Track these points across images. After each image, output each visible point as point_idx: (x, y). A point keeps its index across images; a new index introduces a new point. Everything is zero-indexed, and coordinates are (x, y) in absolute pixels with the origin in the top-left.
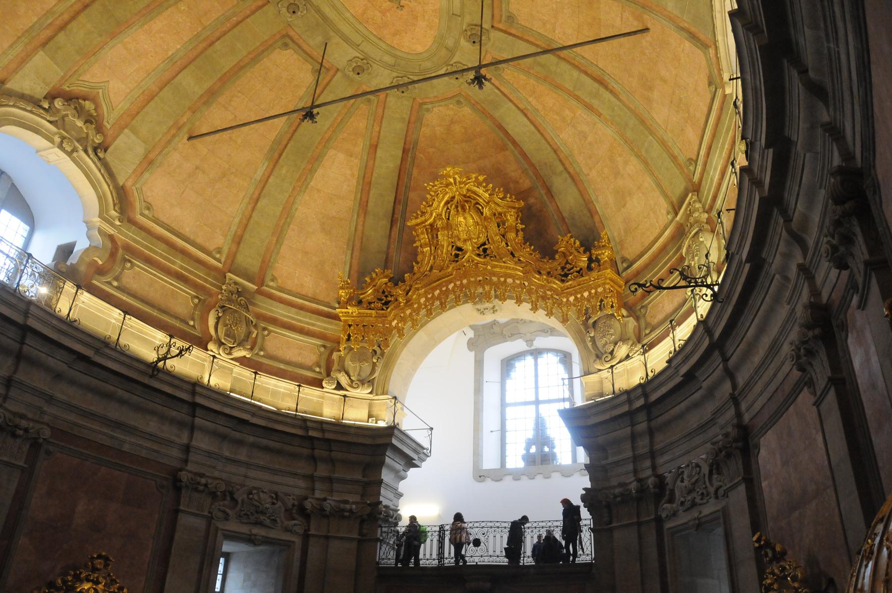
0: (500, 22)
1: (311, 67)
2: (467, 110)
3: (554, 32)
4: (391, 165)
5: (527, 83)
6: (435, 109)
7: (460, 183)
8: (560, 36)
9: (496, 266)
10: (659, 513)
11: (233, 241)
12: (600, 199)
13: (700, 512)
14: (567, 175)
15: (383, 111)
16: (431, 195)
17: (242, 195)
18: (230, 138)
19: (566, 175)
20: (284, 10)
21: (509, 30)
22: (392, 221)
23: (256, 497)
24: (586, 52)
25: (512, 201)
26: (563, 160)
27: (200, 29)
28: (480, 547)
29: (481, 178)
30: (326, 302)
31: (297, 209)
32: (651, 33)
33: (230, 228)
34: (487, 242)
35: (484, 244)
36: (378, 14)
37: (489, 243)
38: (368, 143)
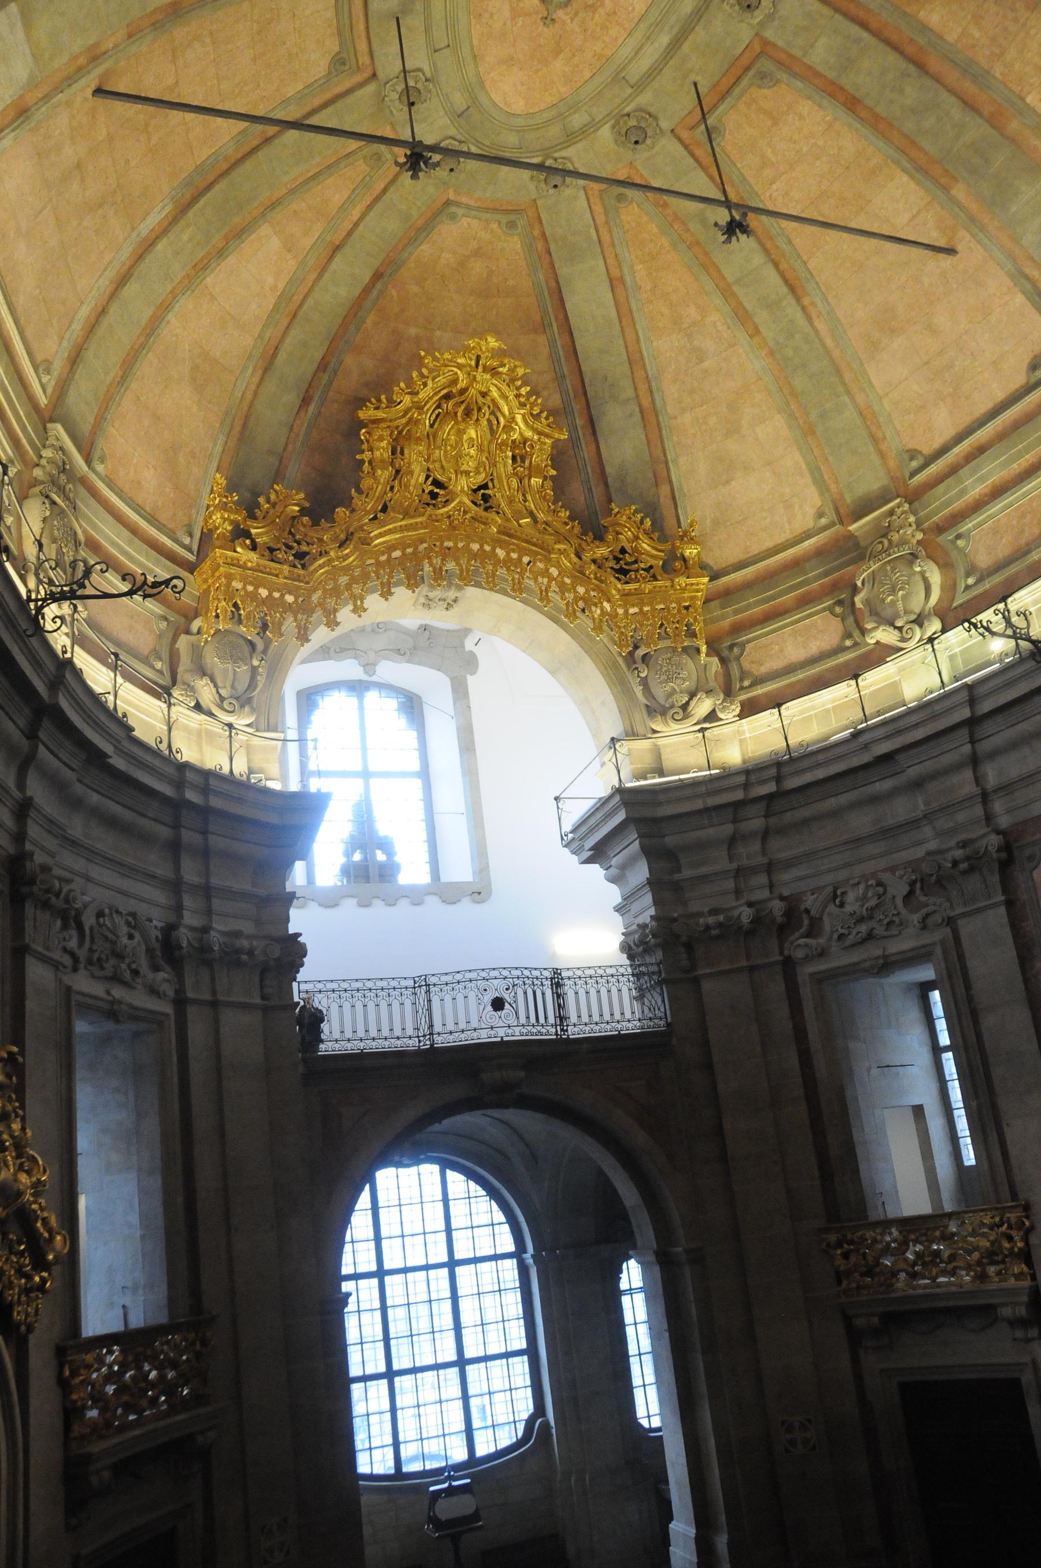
1: (337, 49)
2: (513, 245)
3: (771, 184)
6: (465, 221)
8: (775, 194)
10: (786, 953)
12: (682, 461)
14: (637, 409)
16: (422, 376)
18: (147, 125)
21: (691, 147)
23: (107, 922)
24: (801, 236)
25: (548, 425)
26: (636, 380)
28: (504, 1012)
29: (520, 371)
30: (170, 530)
34: (490, 485)
35: (485, 486)
36: (507, 12)
37: (494, 487)
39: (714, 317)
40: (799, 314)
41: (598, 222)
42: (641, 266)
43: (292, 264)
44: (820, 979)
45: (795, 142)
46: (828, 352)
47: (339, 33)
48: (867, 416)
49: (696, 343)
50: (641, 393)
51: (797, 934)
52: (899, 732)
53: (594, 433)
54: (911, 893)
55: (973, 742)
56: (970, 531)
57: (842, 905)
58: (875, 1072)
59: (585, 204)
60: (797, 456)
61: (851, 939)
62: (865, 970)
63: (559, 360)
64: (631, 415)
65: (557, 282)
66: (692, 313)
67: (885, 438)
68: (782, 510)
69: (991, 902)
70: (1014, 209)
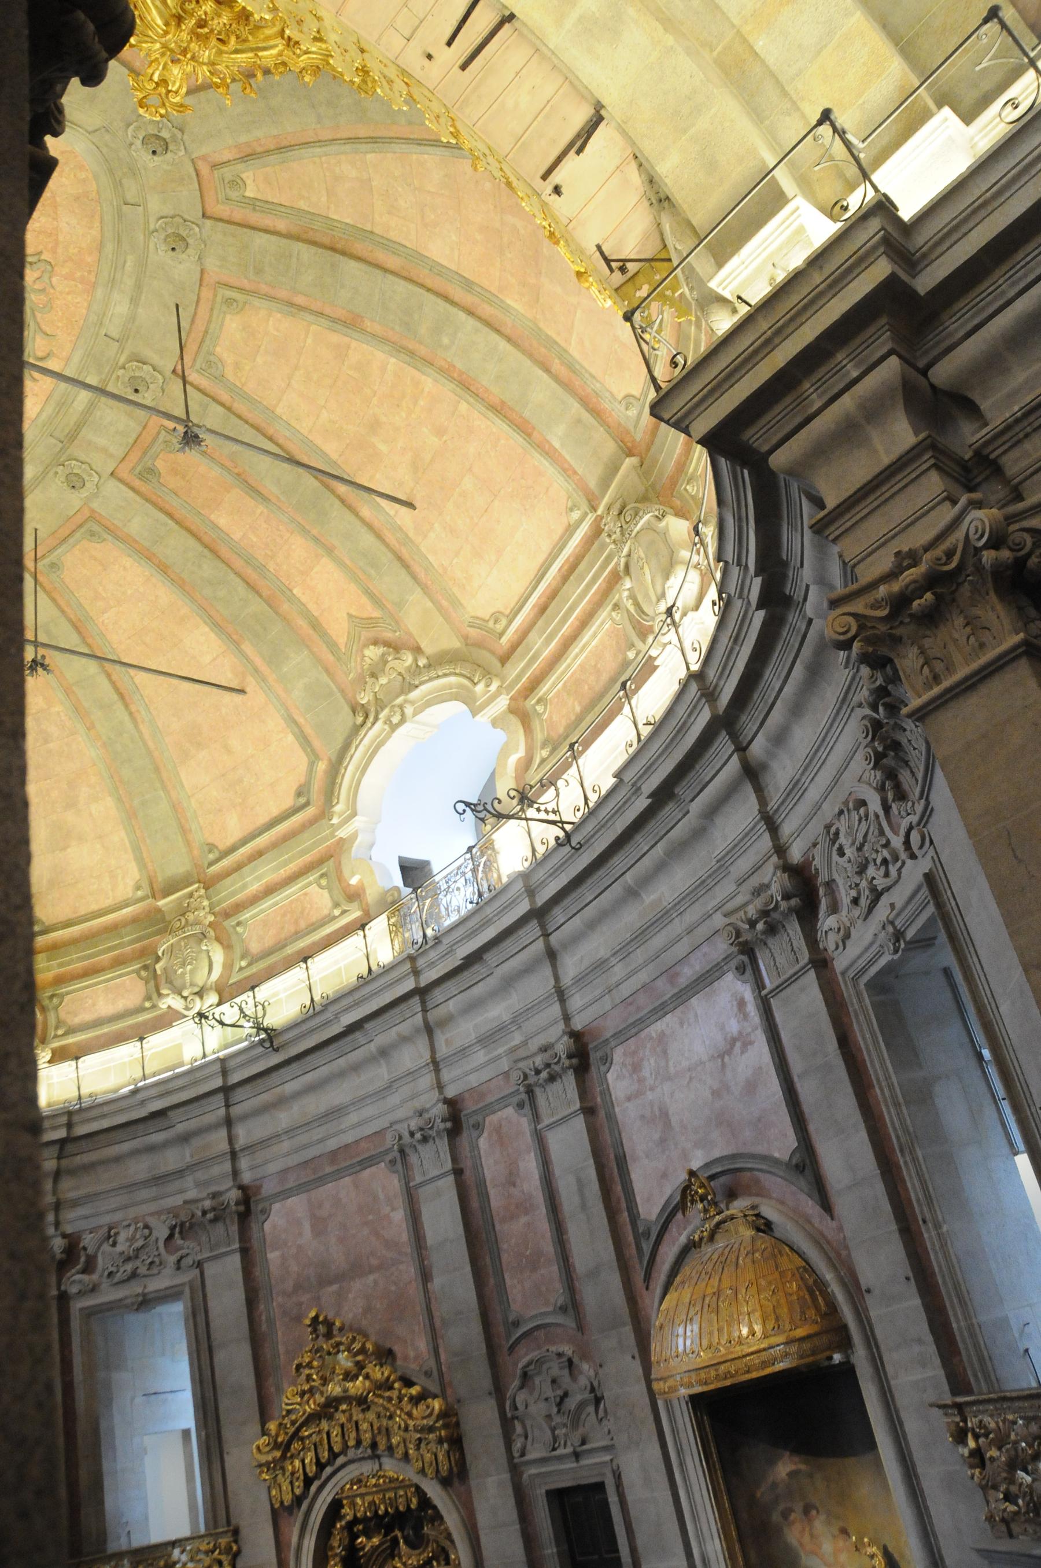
10: (63, 1288)
13: (145, 1287)
39: (57, 708)
40: (127, 718)
44: (89, 1313)
45: (121, 585)
46: (149, 753)
51: (73, 1271)
52: (168, 1093)
54: (170, 1237)
55: (227, 1106)
56: (247, 920)
57: (114, 1244)
58: (139, 1400)
60: (123, 834)
61: (118, 1277)
62: (126, 1306)
69: (228, 1249)
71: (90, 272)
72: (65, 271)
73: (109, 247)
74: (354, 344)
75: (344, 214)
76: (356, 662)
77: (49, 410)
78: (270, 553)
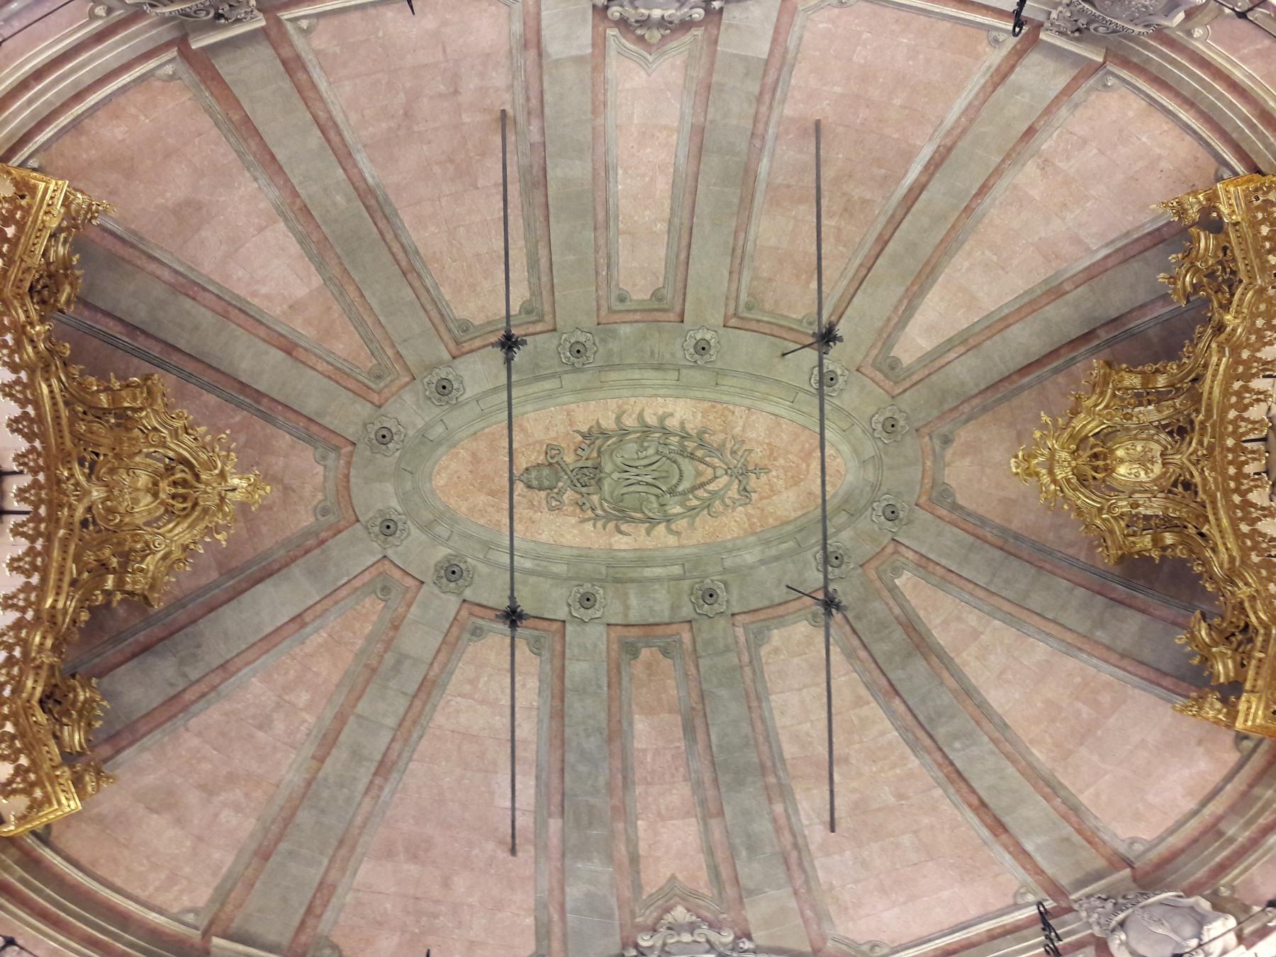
0: (471, 614)
2: (306, 519)
3: (459, 696)
4: (244, 365)
5: (354, 633)
6: (320, 469)
7: (222, 499)
8: (453, 703)
9: (64, 550)
11: (298, 58)
12: (147, 756)
14: (180, 689)
15: (349, 389)
17: (354, 117)
18: (451, 161)
19: (181, 684)
20: (582, 339)
22: (136, 328)
27: (621, 226)
30: (50, 146)
31: (256, 179)
32: (511, 858)
33: (321, 68)
34: (97, 528)
38: (302, 343)
39: (310, 719)
41: (354, 581)
42: (325, 635)
43: (277, 310)
46: (351, 823)
47: (489, 323)
48: (325, 890)
49: (275, 715)
50: (195, 688)
53: (134, 656)
59: (369, 563)
60: (230, 860)
63: (199, 596)
64: (172, 685)
65: (279, 570)
66: (303, 698)
67: (320, 916)
68: (163, 876)
70: (580, 865)
71: (762, 526)
72: (751, 511)
73: (790, 528)
74: (874, 704)
75: (942, 637)
76: (651, 913)
77: (630, 555)
78: (649, 779)
